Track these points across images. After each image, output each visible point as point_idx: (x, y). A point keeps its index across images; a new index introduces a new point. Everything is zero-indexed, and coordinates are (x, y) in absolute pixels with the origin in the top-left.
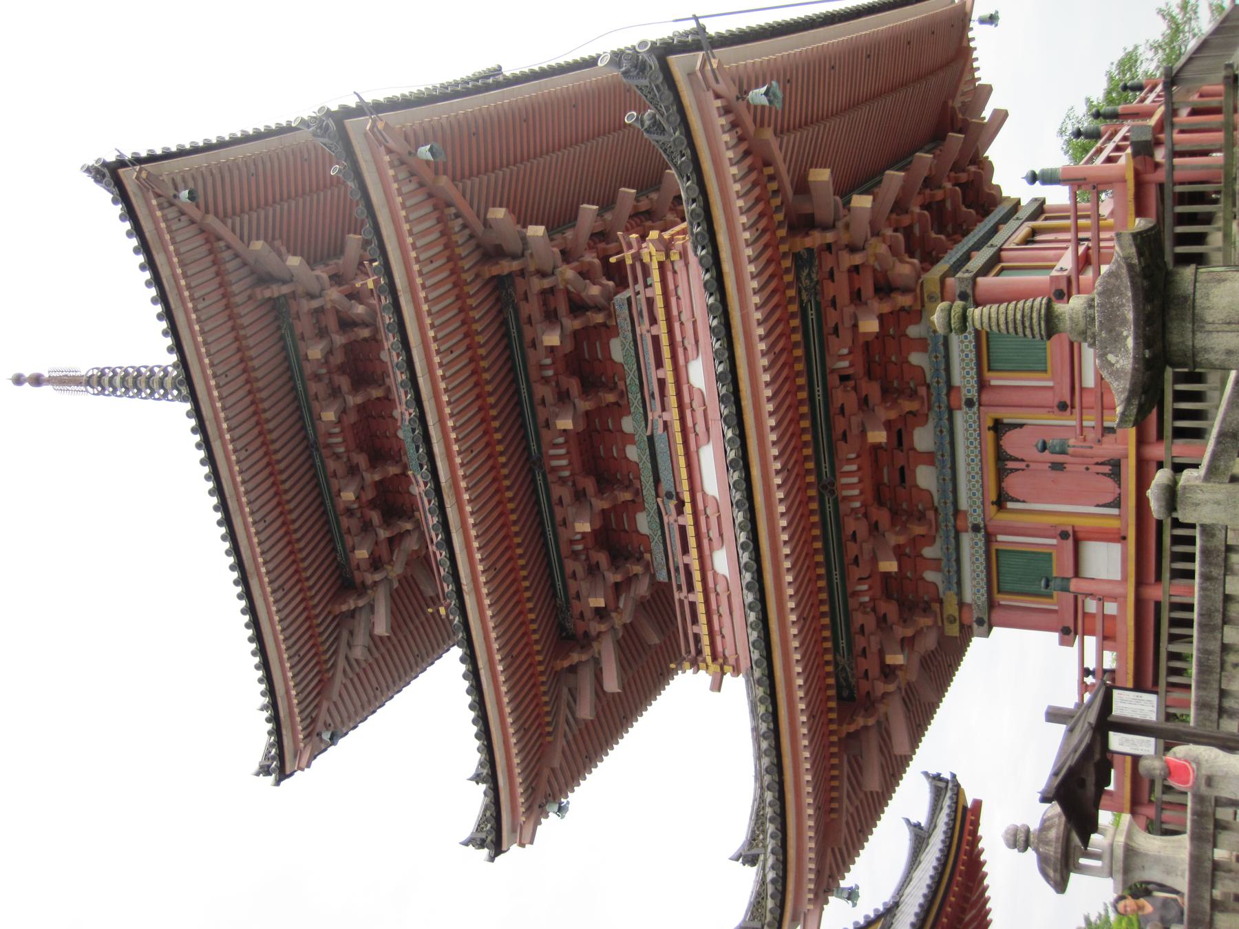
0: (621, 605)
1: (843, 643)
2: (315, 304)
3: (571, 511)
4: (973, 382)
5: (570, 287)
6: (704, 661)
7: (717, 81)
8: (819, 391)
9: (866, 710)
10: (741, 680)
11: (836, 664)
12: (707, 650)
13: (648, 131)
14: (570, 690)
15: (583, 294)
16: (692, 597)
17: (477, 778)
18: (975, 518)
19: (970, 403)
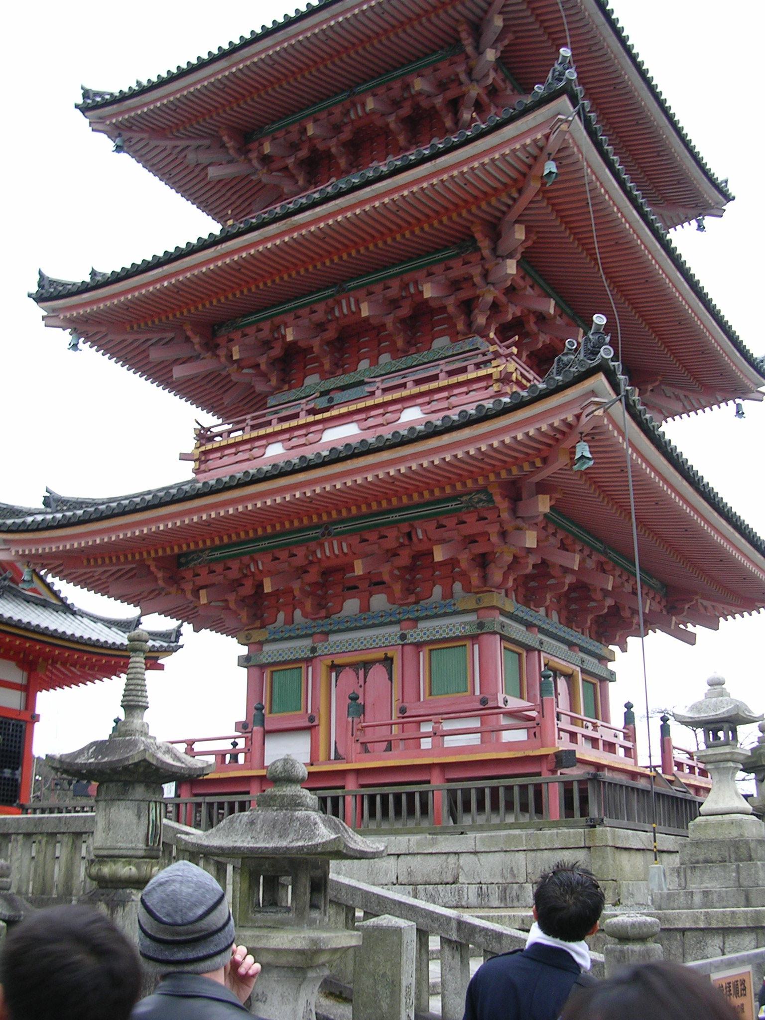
0: (245, 371)
1: (217, 554)
2: (463, 77)
3: (305, 322)
4: (418, 639)
6: (201, 445)
7: (587, 416)
8: (395, 517)
9: (170, 578)
10: (191, 476)
11: (202, 551)
12: (209, 446)
13: (559, 360)
14: (172, 339)
15: (476, 311)
17: (93, 273)
18: (321, 649)
19: (403, 637)
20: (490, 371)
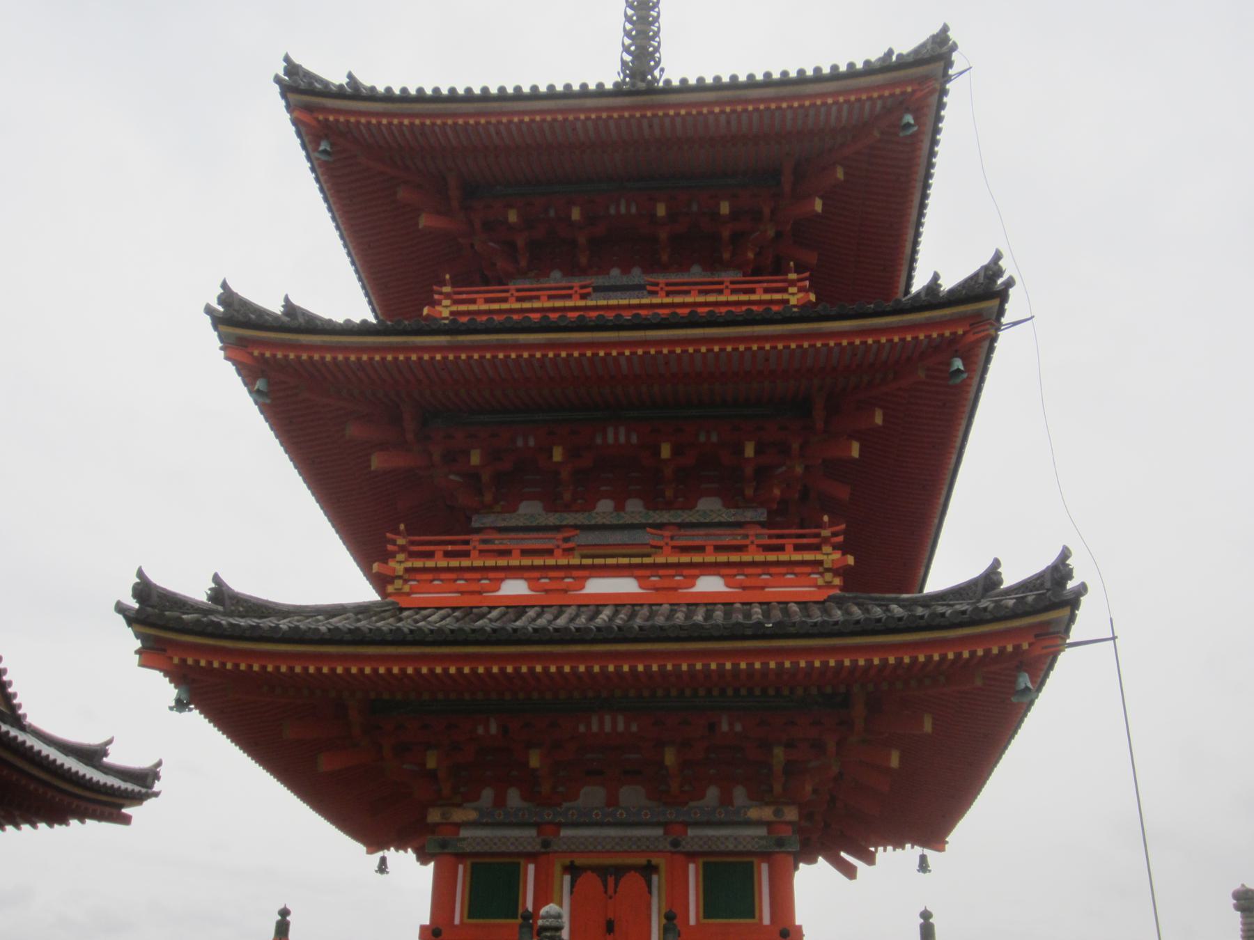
4: (696, 848)
5: (784, 468)
12: (418, 564)
16: (474, 553)
19: (675, 844)
20: (819, 557)
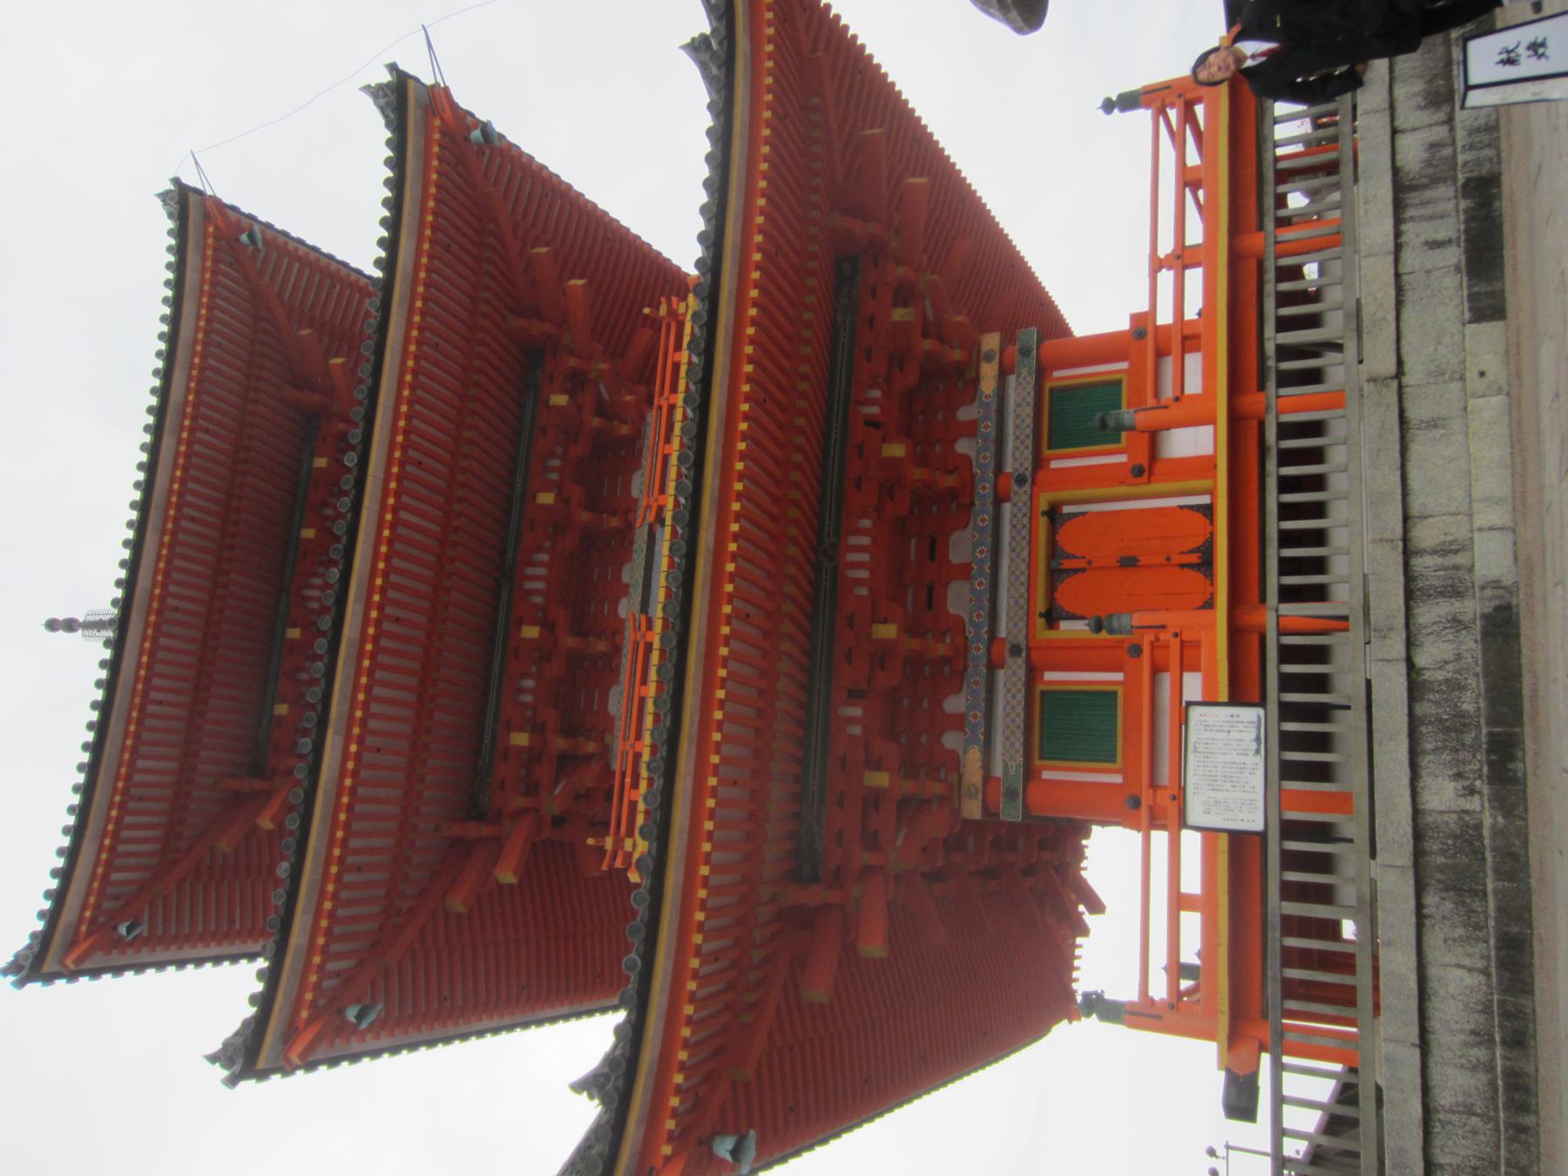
0: (557, 791)
4: (1028, 453)
5: (602, 388)
19: (1021, 480)
